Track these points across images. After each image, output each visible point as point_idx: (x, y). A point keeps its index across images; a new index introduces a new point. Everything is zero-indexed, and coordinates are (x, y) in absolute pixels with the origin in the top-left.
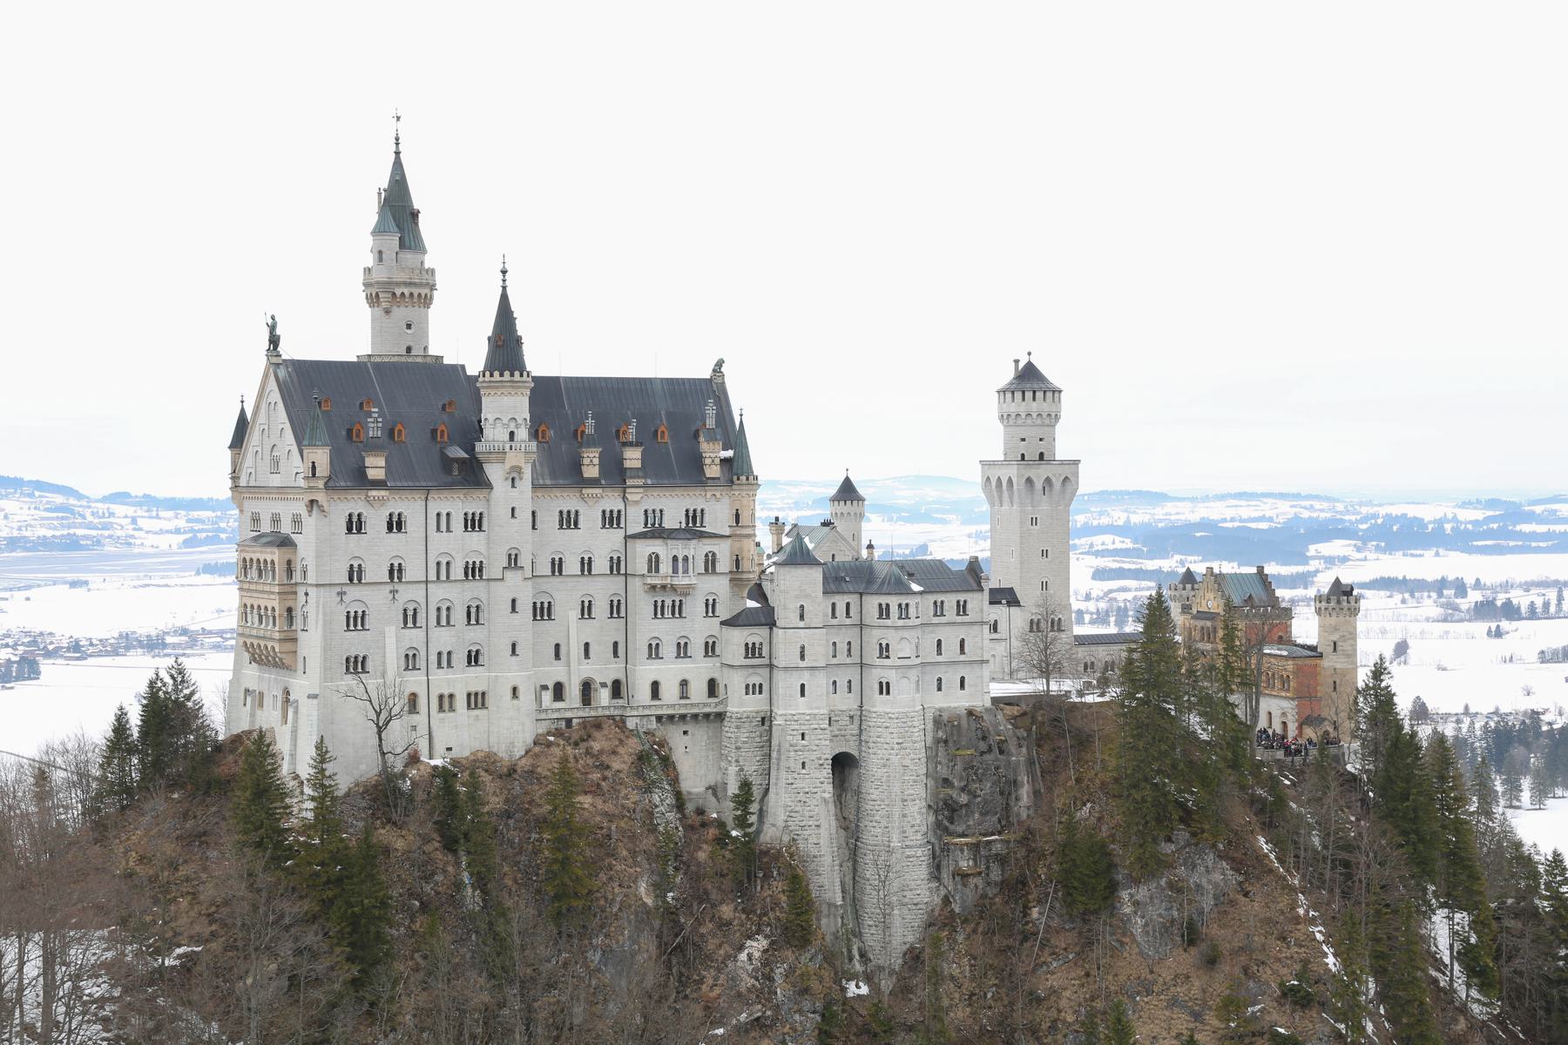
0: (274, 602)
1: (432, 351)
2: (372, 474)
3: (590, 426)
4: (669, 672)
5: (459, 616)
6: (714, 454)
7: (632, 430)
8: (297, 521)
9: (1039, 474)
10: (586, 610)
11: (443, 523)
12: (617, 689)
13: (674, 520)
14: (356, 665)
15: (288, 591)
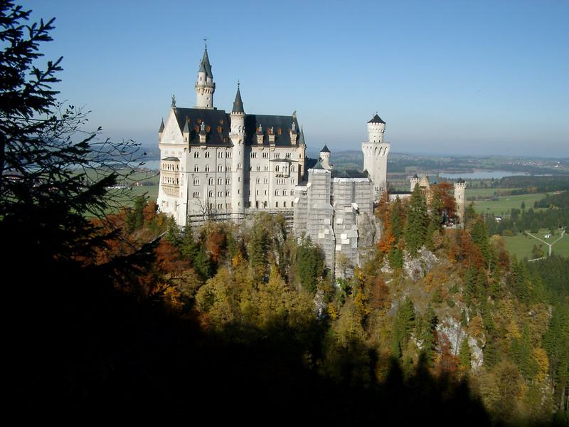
0: (173, 176)
1: (214, 106)
2: (201, 141)
3: (260, 129)
4: (281, 200)
5: (223, 182)
6: (293, 137)
7: (272, 130)
8: (180, 153)
9: (381, 145)
10: (257, 181)
11: (218, 155)
12: (265, 204)
13: (282, 157)
14: (195, 195)
15: (177, 173)
